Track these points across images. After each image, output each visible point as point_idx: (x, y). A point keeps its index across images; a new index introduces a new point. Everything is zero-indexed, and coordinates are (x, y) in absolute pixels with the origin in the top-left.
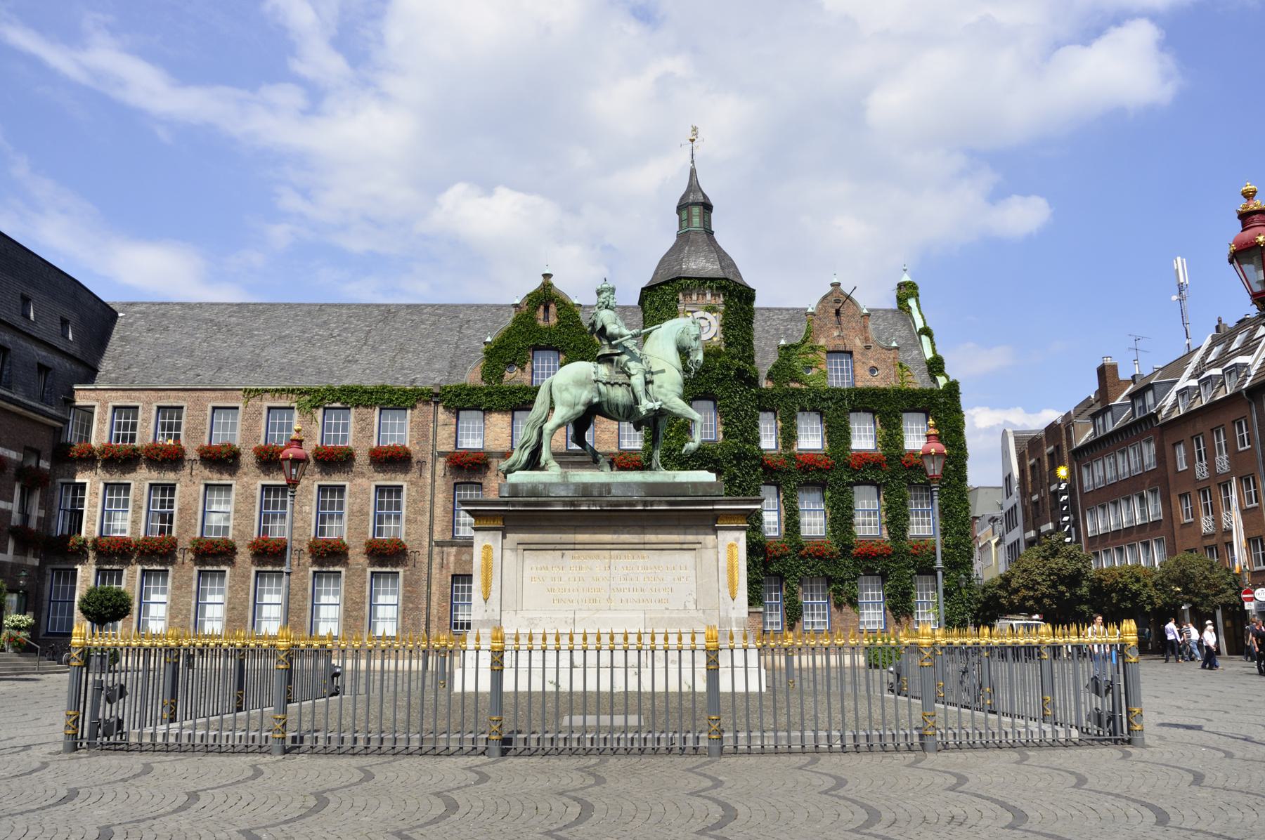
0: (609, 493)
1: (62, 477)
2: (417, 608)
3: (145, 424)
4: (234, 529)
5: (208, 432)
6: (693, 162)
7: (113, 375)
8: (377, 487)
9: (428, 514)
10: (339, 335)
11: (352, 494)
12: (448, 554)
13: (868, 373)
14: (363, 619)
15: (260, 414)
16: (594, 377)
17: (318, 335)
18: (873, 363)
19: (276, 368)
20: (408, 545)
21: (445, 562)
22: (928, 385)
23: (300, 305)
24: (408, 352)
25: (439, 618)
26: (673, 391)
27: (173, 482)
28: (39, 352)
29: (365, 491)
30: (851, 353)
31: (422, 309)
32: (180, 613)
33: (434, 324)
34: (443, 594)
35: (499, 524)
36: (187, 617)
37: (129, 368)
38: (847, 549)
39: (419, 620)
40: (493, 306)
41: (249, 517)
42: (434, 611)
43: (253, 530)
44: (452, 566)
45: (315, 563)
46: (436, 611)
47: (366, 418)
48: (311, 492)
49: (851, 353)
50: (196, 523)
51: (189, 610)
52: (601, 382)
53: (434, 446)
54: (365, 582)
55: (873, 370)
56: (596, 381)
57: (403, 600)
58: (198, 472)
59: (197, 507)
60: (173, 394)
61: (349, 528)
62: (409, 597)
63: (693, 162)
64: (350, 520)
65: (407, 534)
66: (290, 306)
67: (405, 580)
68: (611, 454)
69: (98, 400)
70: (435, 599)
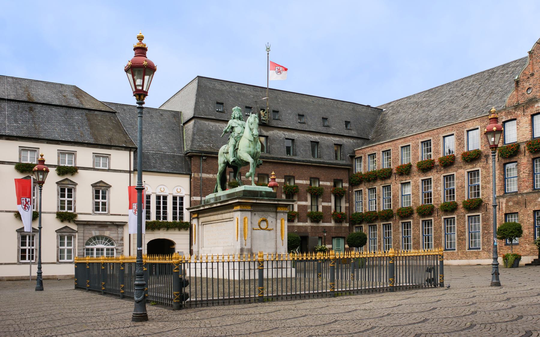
1: (355, 189)
2: (489, 233)
3: (379, 160)
4: (412, 202)
8: (468, 172)
11: (458, 178)
15: (418, 146)
17: (457, 96)
19: (433, 119)
20: (483, 200)
23: (453, 82)
27: (389, 184)
28: (335, 139)
29: (463, 176)
31: (509, 65)
37: (380, 135)
41: (418, 196)
43: (419, 202)
47: (461, 138)
48: (440, 180)
59: (399, 194)
61: (457, 196)
65: (483, 195)
66: (449, 84)
67: (483, 219)
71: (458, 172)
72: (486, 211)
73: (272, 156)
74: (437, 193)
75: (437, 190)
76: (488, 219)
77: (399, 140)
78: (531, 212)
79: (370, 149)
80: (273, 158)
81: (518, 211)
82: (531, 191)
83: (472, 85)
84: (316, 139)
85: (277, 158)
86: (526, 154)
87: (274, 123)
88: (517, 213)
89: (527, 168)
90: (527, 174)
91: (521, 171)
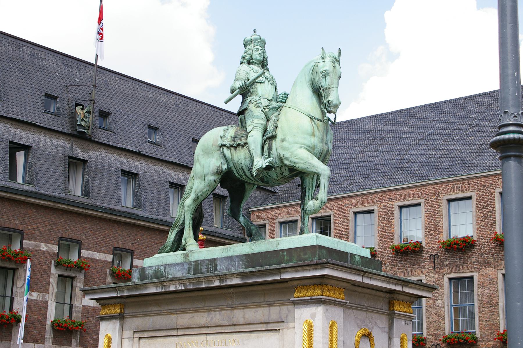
7: (287, 195)
10: (477, 125)
11: (481, 285)
15: (393, 214)
16: (219, 143)
17: (458, 128)
19: (415, 166)
26: (296, 143)
29: (493, 282)
35: (117, 311)
52: (225, 146)
56: (222, 146)
61: (480, 321)
64: (480, 312)
69: (268, 219)
71: (481, 272)
73: (95, 202)
74: (434, 311)
75: (434, 307)
77: (349, 199)
79: (283, 210)
80: (94, 208)
83: (489, 111)
84: (180, 179)
85: (102, 208)
87: (102, 136)
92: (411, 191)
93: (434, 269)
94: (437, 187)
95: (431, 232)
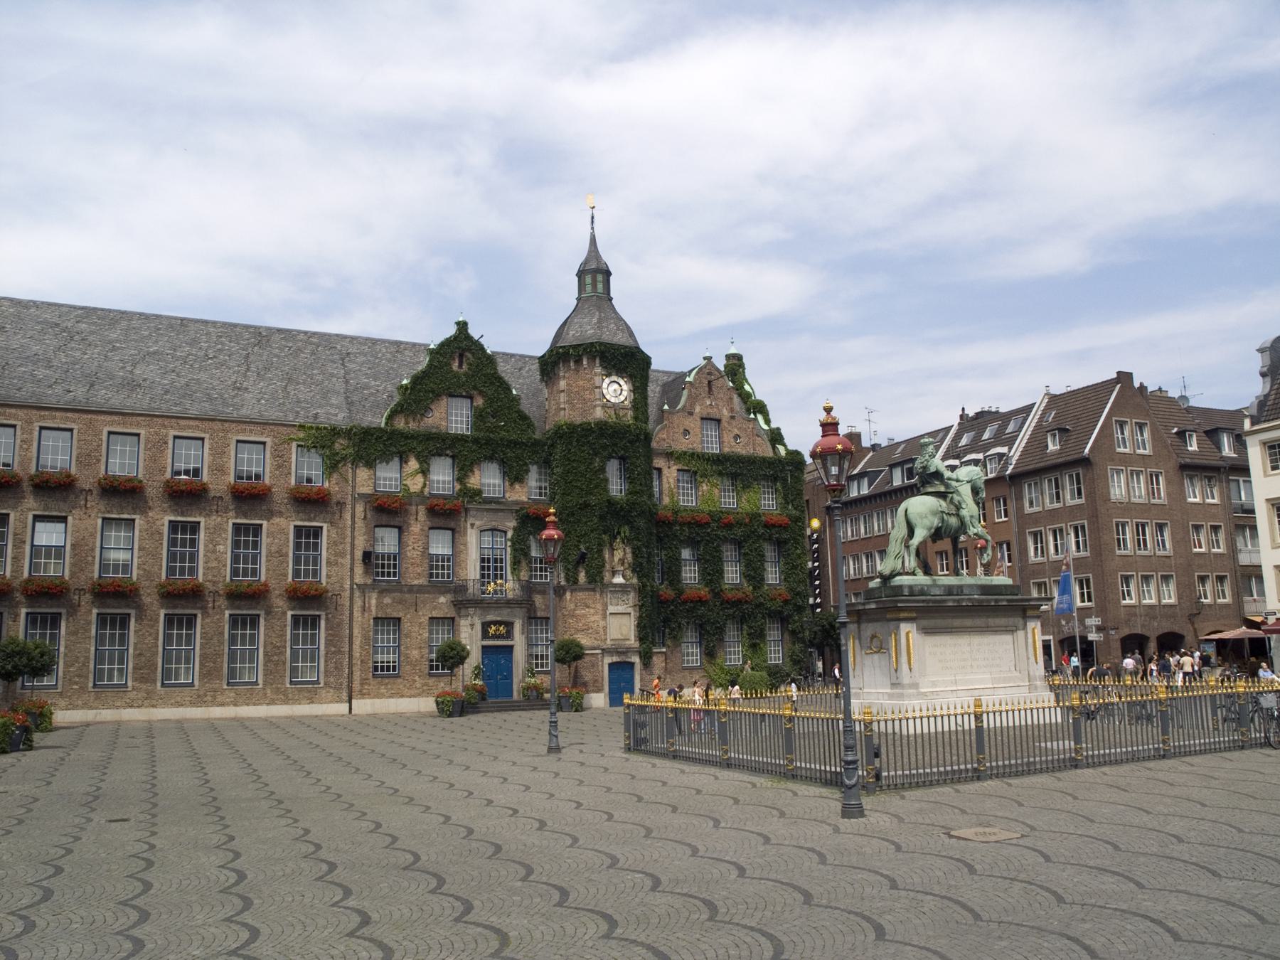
0: (962, 591)
2: (340, 652)
3: (25, 446)
4: (138, 568)
5: (104, 460)
6: (592, 228)
9: (349, 557)
12: (370, 598)
13: (732, 440)
14: (284, 663)
15: (166, 443)
18: (736, 431)
21: (367, 605)
22: (769, 453)
24: (298, 384)
25: (362, 661)
27: (64, 514)
29: (283, 532)
30: (719, 421)
32: (76, 662)
33: (313, 353)
34: (366, 637)
36: (85, 664)
38: (717, 593)
39: (341, 663)
40: (367, 339)
41: (156, 556)
42: (356, 654)
43: (160, 569)
44: (373, 609)
45: (231, 607)
46: (358, 654)
48: (225, 531)
49: (719, 421)
50: (93, 561)
51: (87, 658)
53: (354, 487)
54: (285, 626)
55: (737, 437)
57: (326, 643)
58: (93, 503)
59: (94, 543)
60: (58, 414)
61: (268, 570)
62: (331, 640)
63: (592, 228)
64: (268, 561)
65: (328, 576)
68: (523, 503)
70: (357, 642)
71: (272, 521)
72: (336, 609)
74: (213, 556)
75: (214, 552)
76: (340, 624)
78: (425, 620)
81: (400, 615)
82: (426, 583)
86: (419, 519)
88: (399, 619)
89: (420, 543)
90: (419, 553)
91: (408, 546)
92: (192, 423)
93: (217, 512)
94: (226, 425)
95: (215, 472)
